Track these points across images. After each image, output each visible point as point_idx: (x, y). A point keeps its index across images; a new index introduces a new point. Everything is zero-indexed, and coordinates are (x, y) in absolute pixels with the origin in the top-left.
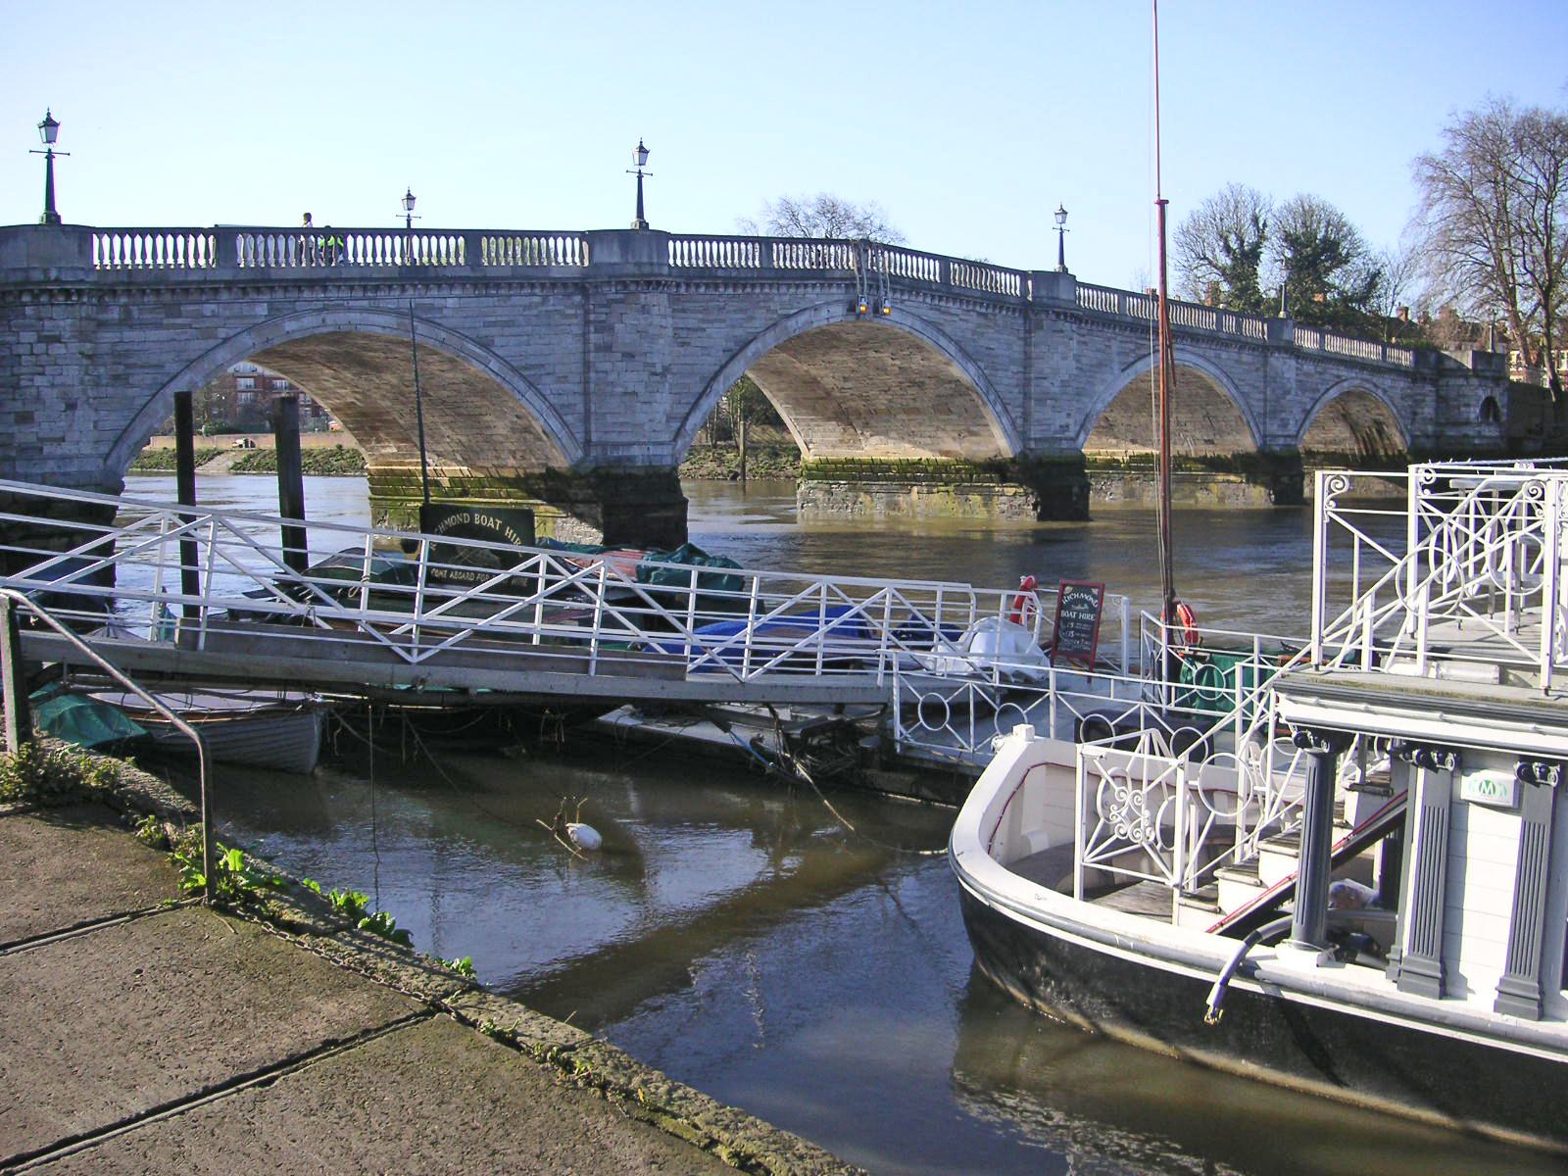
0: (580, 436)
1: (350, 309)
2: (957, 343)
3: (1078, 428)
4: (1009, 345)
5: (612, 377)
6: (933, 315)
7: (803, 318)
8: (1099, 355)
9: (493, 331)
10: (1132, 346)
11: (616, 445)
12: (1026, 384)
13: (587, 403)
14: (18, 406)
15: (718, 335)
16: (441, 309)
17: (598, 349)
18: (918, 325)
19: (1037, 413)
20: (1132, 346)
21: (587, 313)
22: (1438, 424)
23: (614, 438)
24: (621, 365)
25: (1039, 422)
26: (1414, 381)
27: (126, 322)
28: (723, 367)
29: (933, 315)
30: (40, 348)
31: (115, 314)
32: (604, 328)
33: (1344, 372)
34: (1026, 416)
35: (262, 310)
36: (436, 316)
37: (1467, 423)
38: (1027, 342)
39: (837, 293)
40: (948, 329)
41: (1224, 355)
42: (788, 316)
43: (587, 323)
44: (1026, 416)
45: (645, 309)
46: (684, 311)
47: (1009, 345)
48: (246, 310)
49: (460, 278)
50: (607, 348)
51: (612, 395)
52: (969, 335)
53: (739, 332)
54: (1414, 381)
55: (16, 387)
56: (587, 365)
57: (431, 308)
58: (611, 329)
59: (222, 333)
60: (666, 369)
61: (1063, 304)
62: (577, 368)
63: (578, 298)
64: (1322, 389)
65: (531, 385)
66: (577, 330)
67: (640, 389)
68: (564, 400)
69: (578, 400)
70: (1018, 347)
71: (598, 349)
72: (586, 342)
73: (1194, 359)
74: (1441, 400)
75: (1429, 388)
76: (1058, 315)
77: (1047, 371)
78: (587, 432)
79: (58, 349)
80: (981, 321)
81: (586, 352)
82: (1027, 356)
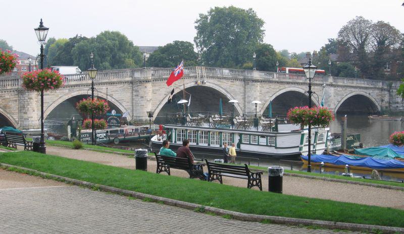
0: (131, 115)
1: (84, 90)
2: (225, 89)
3: (260, 109)
4: (240, 89)
5: (138, 102)
6: (219, 83)
8: (268, 90)
9: (113, 93)
10: (278, 87)
11: (139, 117)
13: (133, 107)
14: (24, 111)
16: (102, 89)
17: (135, 96)
18: (214, 86)
20: (278, 87)
21: (133, 88)
22: (390, 103)
23: (138, 115)
24: (140, 99)
25: (249, 108)
26: (382, 90)
28: (164, 98)
29: (219, 83)
30: (29, 100)
32: (137, 91)
33: (353, 90)
34: (245, 106)
35: (67, 91)
36: (101, 91)
37: (398, 103)
38: (245, 87)
39: (193, 80)
43: (133, 90)
44: (245, 106)
46: (155, 86)
48: (64, 91)
49: (106, 82)
50: (138, 96)
51: (138, 106)
52: (228, 87)
54: (382, 90)
55: (24, 107)
56: (133, 99)
57: (100, 89)
58: (138, 91)
59: (60, 96)
60: (151, 100)
61: (254, 78)
62: (130, 100)
63: (131, 85)
64: (345, 94)
65: (121, 104)
66: (131, 92)
67: (144, 104)
68: (128, 107)
69: (131, 107)
70: (242, 89)
71: (135, 96)
72: (133, 94)
73: (298, 89)
74: (390, 95)
75: (386, 92)
76: (253, 81)
77: (250, 95)
78: (133, 113)
79: (31, 100)
80: (232, 83)
81: (133, 96)
82: (245, 92)
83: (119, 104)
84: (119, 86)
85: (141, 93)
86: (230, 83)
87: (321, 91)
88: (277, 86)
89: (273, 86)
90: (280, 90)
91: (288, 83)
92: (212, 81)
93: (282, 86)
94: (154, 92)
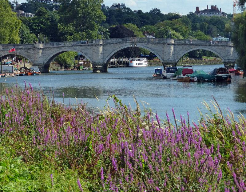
2: (151, 49)
7: (123, 47)
8: (181, 49)
12: (163, 53)
15: (111, 49)
19: (165, 57)
27: (46, 51)
31: (45, 50)
39: (129, 44)
40: (149, 47)
41: (213, 47)
42: (121, 47)
45: (97, 47)
47: (161, 48)
50: (94, 51)
52: (153, 47)
53: (114, 49)
57: (75, 48)
80: (155, 45)
83: (85, 55)
84: (85, 47)
85: (96, 50)
86: (154, 45)
87: (223, 49)
88: (188, 47)
89: (185, 47)
90: (190, 49)
91: (197, 45)
92: (142, 44)
93: (192, 47)
94: (103, 50)
